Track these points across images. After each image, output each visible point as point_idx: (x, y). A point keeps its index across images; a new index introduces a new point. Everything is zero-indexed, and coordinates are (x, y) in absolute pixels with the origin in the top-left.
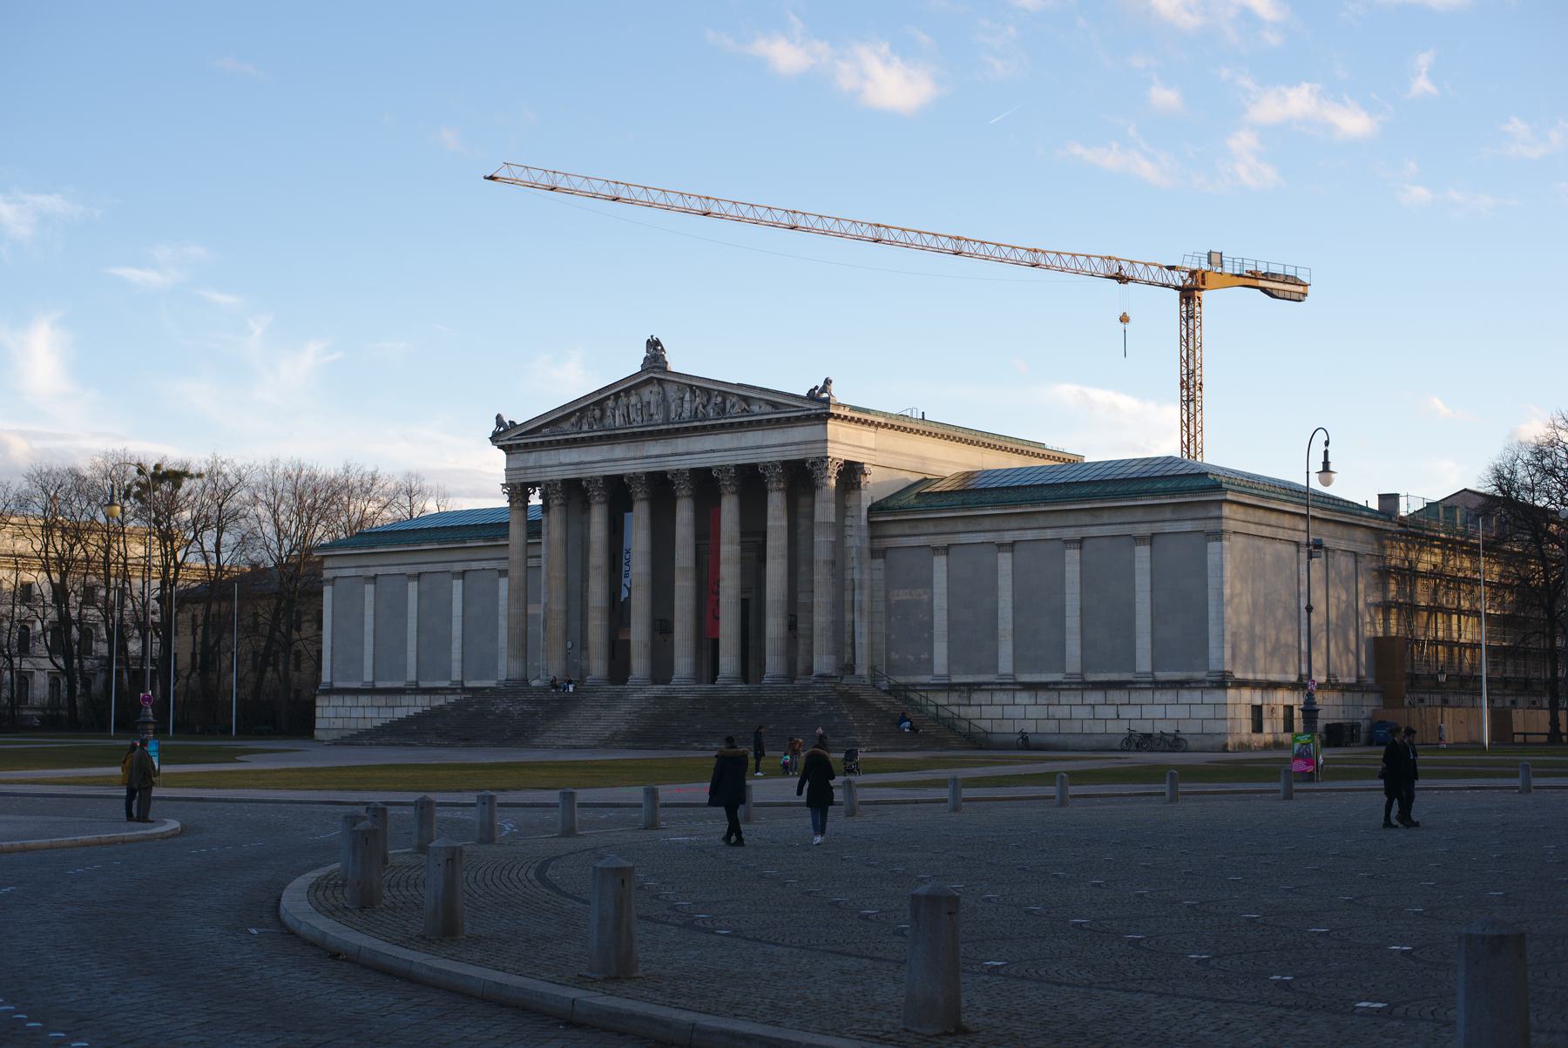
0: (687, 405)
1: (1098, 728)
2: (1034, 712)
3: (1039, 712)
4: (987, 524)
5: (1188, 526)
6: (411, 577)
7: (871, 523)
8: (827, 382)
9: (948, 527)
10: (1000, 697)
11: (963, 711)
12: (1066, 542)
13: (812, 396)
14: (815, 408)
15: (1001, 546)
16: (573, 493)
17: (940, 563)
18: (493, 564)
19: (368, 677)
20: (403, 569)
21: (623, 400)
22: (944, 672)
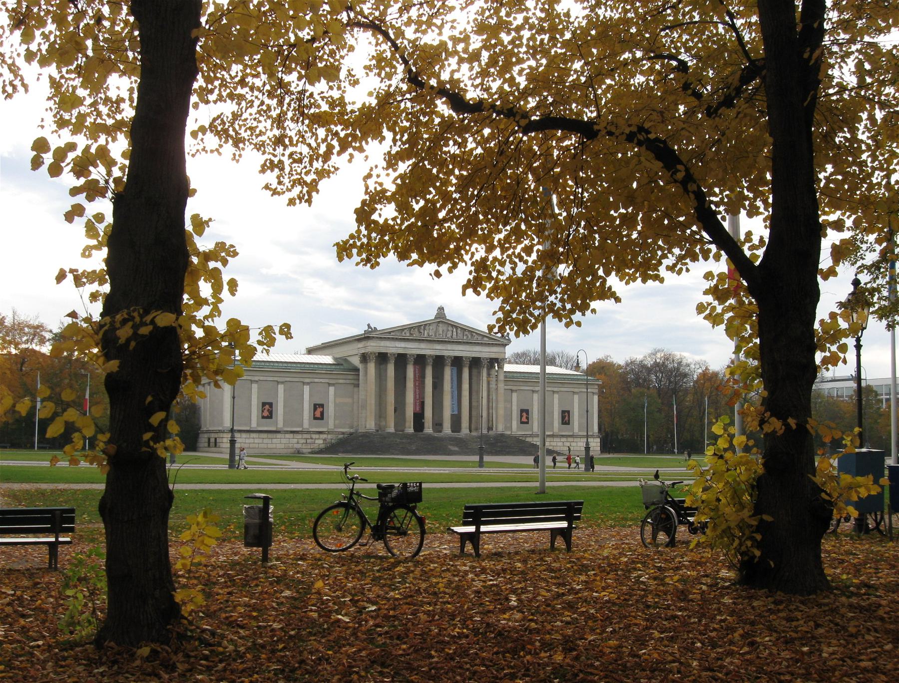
0: (455, 333)
4: (530, 384)
9: (518, 384)
18: (327, 381)
21: (427, 327)
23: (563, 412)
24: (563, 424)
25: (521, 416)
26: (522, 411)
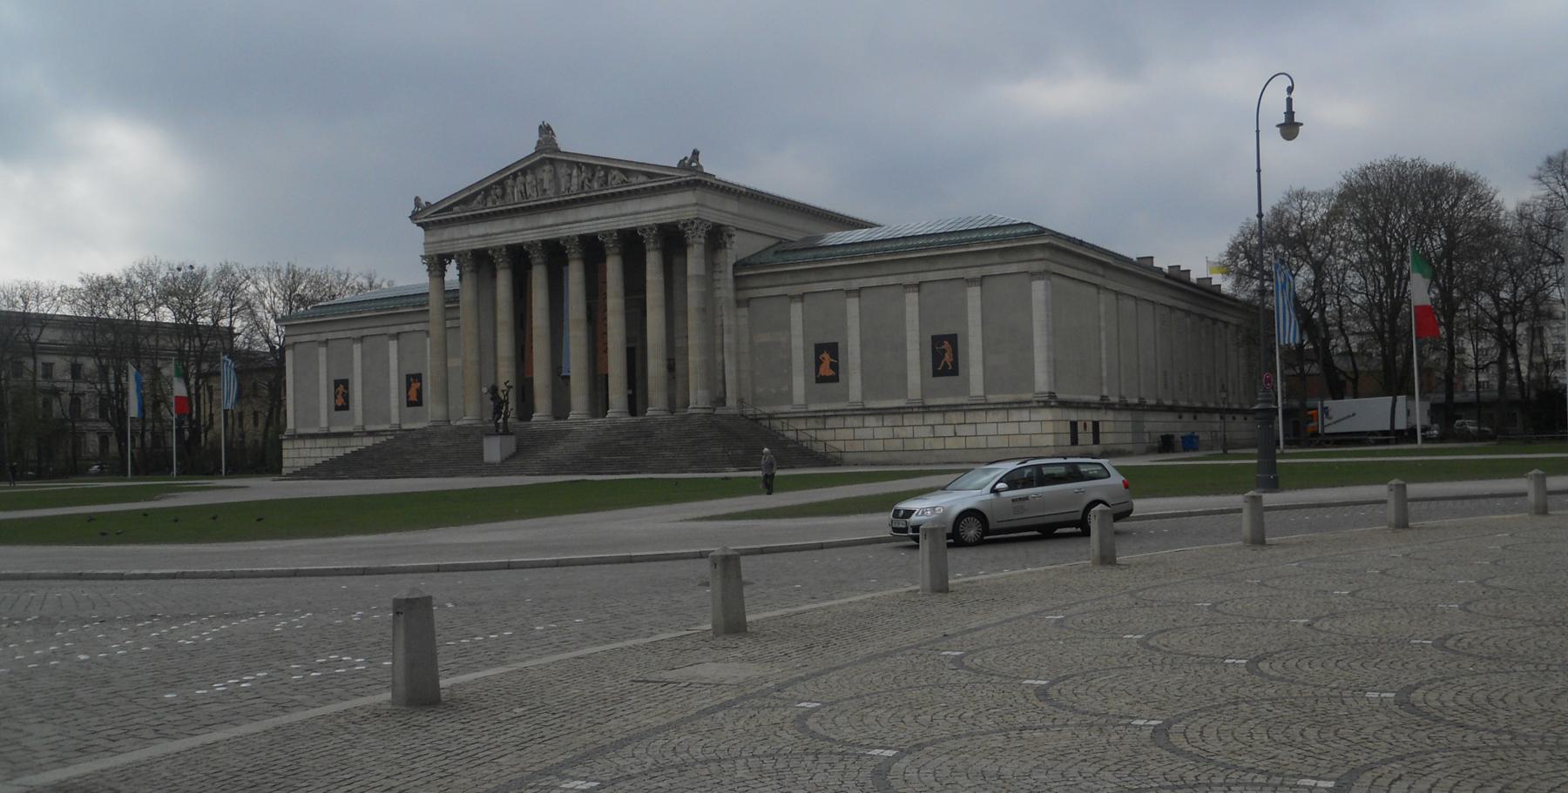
0: (575, 181)
1: (938, 444)
2: (880, 433)
3: (887, 433)
4: (837, 274)
5: (1014, 268)
6: (354, 340)
7: (736, 278)
8: (696, 153)
10: (850, 421)
11: (822, 435)
12: (906, 286)
13: (683, 165)
14: (685, 176)
15: (849, 292)
16: (480, 262)
17: (796, 310)
19: (324, 423)
20: (349, 334)
21: (520, 179)
22: (802, 402)
23: (937, 340)
24: (936, 373)
25: (818, 363)
26: (820, 348)
